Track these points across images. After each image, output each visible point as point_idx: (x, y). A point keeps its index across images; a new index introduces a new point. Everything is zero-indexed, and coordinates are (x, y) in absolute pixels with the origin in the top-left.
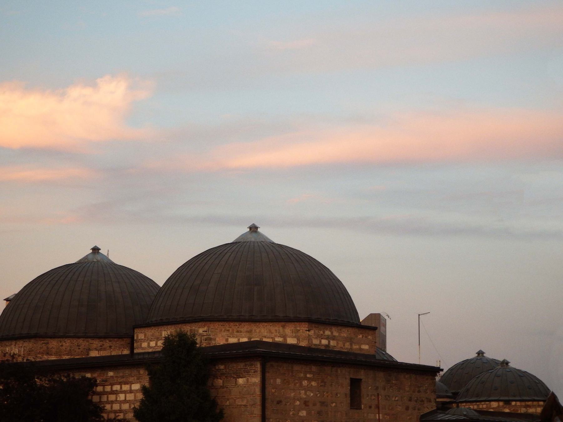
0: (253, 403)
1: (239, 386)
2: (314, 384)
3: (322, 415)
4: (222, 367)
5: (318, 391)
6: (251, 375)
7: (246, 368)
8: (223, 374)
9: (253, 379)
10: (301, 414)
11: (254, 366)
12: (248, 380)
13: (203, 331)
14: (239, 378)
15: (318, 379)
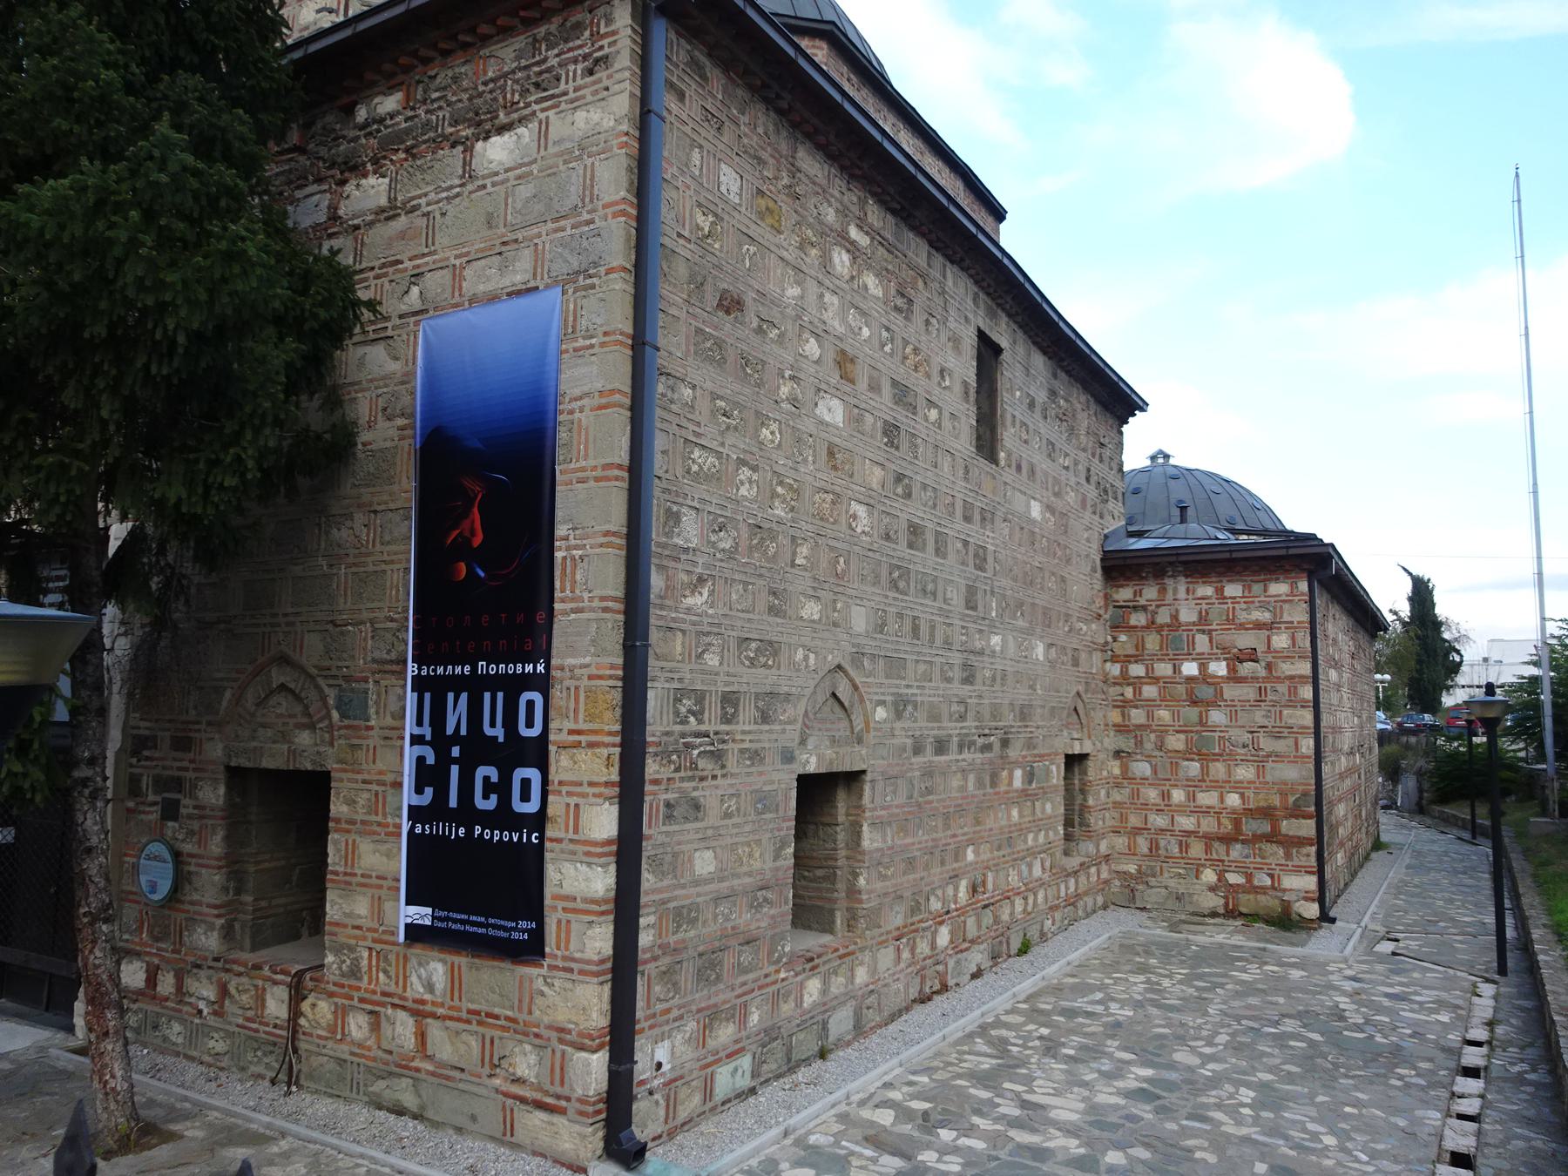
0: (575, 266)
1: (488, 182)
2: (870, 280)
3: (897, 448)
4: (389, 104)
5: (888, 329)
6: (565, 93)
7: (538, 63)
8: (391, 143)
9: (581, 115)
10: (825, 411)
11: (587, 33)
12: (543, 135)
13: (318, 11)
14: (486, 138)
15: (887, 270)
